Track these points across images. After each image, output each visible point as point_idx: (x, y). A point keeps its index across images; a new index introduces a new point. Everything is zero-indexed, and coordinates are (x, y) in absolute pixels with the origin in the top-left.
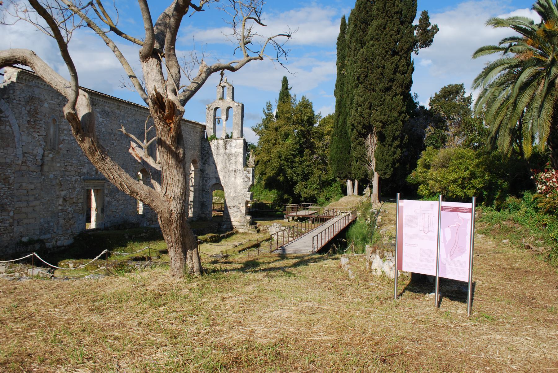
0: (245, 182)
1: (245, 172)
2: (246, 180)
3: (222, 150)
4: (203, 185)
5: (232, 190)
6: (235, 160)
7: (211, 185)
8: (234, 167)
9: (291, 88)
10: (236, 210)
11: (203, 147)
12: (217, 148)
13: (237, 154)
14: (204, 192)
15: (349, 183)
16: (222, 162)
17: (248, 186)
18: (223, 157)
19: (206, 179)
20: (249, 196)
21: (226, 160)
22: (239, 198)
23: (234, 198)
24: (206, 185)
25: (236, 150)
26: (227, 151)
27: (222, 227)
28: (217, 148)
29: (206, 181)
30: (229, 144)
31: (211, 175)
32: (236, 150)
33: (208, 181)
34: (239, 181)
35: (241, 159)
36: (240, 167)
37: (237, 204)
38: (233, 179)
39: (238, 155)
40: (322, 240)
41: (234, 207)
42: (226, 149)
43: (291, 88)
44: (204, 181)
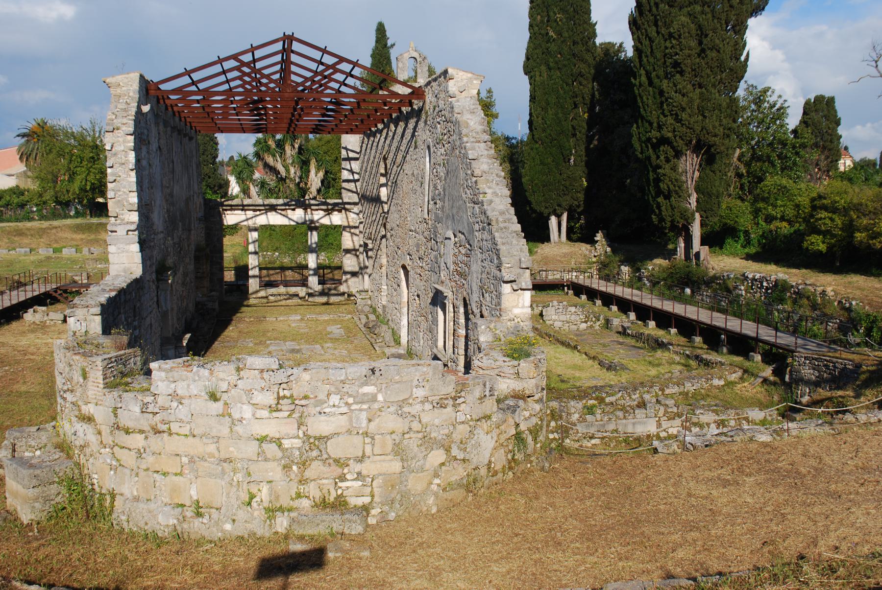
9: (394, 45)
43: (394, 45)
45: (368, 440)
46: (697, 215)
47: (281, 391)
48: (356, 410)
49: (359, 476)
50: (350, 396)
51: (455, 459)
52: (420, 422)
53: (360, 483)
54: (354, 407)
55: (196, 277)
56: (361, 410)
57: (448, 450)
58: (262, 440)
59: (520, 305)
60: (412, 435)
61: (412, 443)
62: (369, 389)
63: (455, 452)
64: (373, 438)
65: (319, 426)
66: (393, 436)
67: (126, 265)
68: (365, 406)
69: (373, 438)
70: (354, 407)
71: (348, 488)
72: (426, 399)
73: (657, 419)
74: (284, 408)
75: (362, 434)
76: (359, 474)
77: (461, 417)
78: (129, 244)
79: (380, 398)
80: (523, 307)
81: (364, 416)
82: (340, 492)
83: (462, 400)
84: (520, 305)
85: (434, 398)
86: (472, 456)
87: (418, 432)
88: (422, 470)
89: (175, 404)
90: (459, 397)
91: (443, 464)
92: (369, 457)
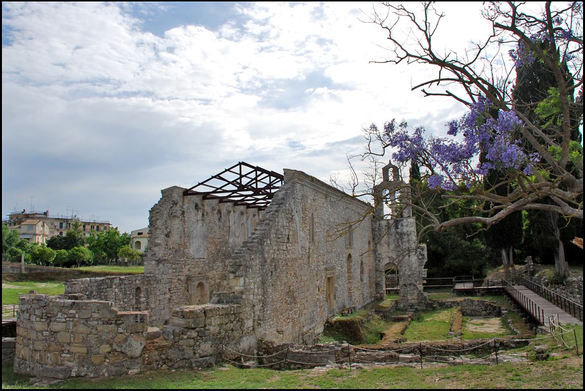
0: (420, 259)
2: (421, 257)
3: (393, 230)
4: (376, 265)
5: (407, 268)
6: (407, 239)
7: (384, 265)
8: (407, 245)
10: (412, 287)
11: (373, 227)
13: (409, 232)
14: (378, 272)
15: (504, 253)
16: (394, 241)
18: (395, 236)
19: (379, 259)
20: (426, 273)
21: (398, 239)
22: (415, 275)
23: (409, 276)
24: (379, 265)
25: (408, 229)
26: (399, 230)
27: (399, 305)
30: (400, 224)
31: (384, 255)
32: (408, 229)
33: (381, 260)
34: (414, 258)
37: (413, 282)
39: (410, 234)
40: (539, 313)
41: (410, 285)
44: (377, 261)
45: (72, 335)
46: (561, 243)
50: (66, 314)
53: (69, 355)
54: (67, 319)
56: (69, 321)
57: (111, 345)
60: (92, 335)
61: (93, 340)
63: (115, 347)
64: (74, 335)
65: (56, 327)
66: (83, 335)
67: (151, 270)
68: (71, 319)
69: (74, 335)
70: (67, 319)
71: (65, 357)
76: (69, 351)
78: (151, 261)
80: (240, 286)
81: (71, 323)
84: (238, 285)
85: (104, 319)
86: (127, 351)
88: (99, 354)
90: (119, 320)
91: (109, 353)
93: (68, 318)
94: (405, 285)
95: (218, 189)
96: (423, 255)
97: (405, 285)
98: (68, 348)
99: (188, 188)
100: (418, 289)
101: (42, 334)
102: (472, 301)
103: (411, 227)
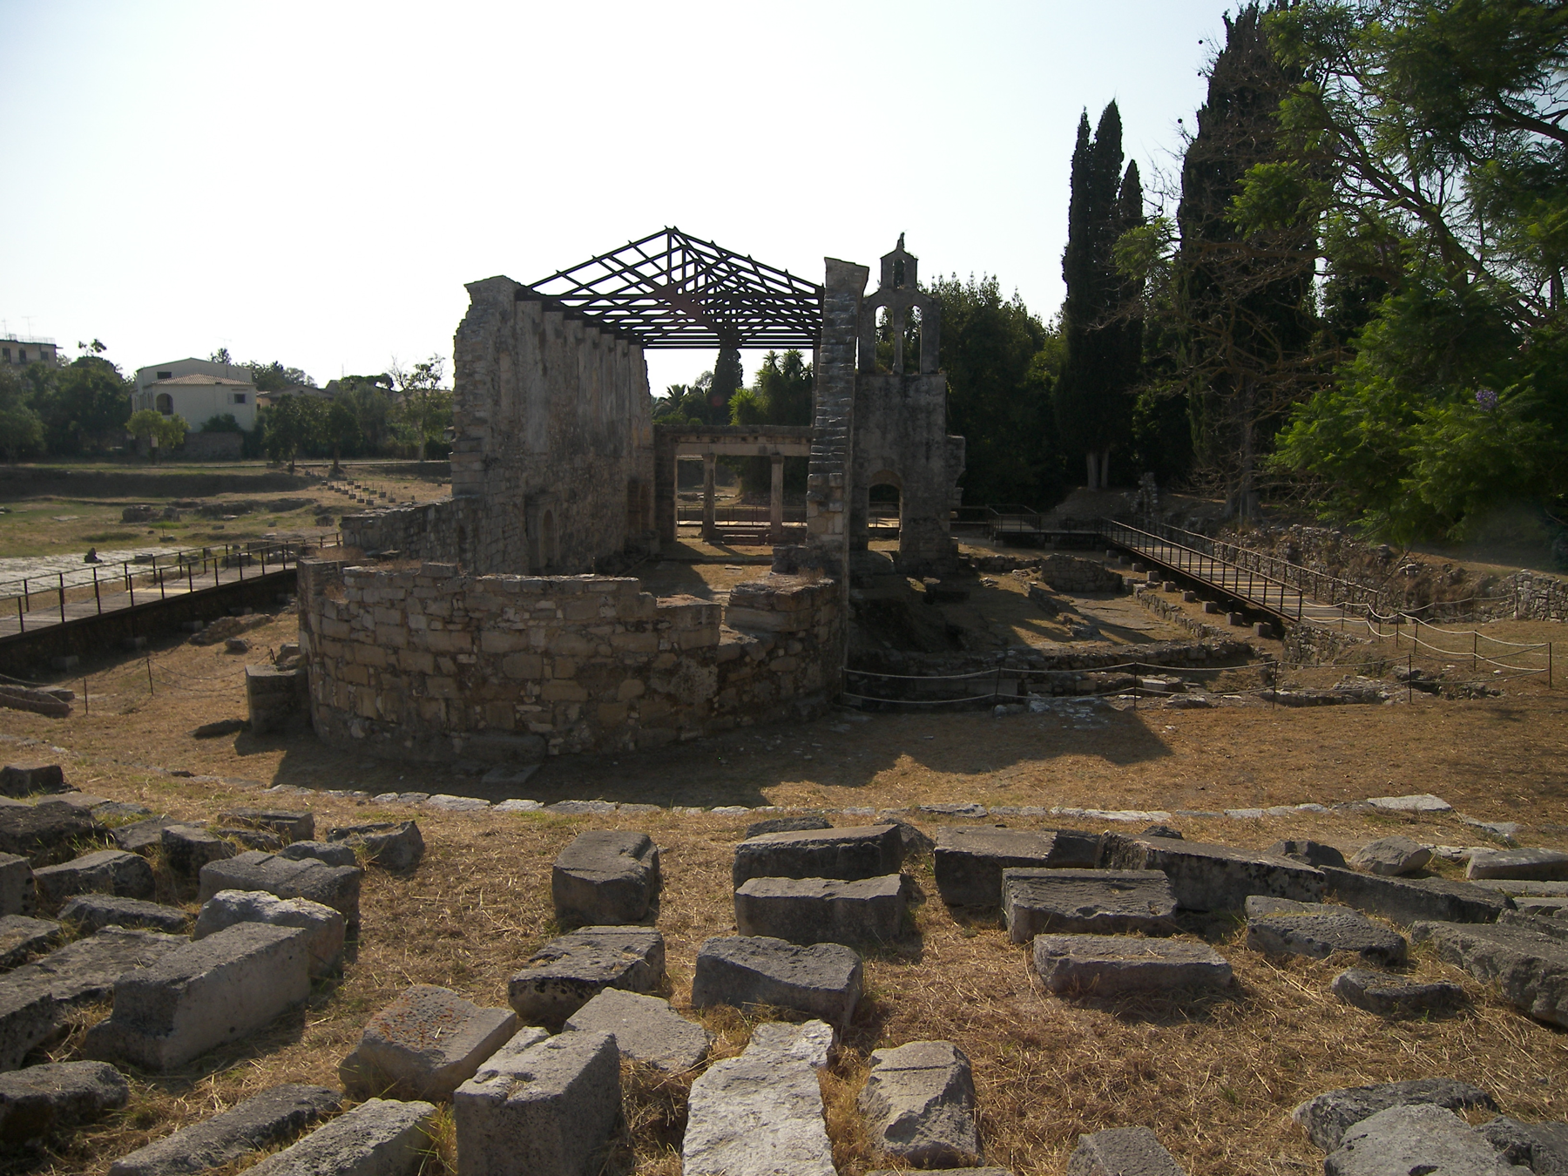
0: (950, 466)
1: (950, 447)
2: (953, 462)
3: (897, 400)
12: (886, 395)
17: (957, 477)
20: (959, 496)
28: (886, 395)
29: (861, 466)
30: (913, 387)
33: (866, 464)
34: (937, 464)
35: (940, 419)
36: (938, 436)
38: (923, 461)
41: (925, 520)
42: (907, 396)
47: (455, 601)
48: (534, 626)
49: (539, 700)
50: (527, 611)
51: (655, 691)
52: (610, 645)
53: (540, 708)
55: (630, 511)
58: (438, 654)
59: (830, 531)
62: (543, 604)
68: (543, 623)
71: (526, 712)
72: (618, 621)
73: (1020, 681)
74: (457, 620)
75: (541, 654)
76: (538, 697)
77: (665, 645)
79: (560, 614)
82: (518, 716)
83: (665, 625)
84: (830, 531)
87: (607, 657)
88: (614, 700)
89: (362, 611)
90: (662, 622)
92: (548, 680)
93: (535, 619)
94: (915, 520)
95: (581, 287)
96: (957, 458)
97: (915, 520)
98: (536, 690)
99: (527, 283)
100: (940, 529)
101: (454, 660)
102: (1070, 561)
103: (937, 395)
